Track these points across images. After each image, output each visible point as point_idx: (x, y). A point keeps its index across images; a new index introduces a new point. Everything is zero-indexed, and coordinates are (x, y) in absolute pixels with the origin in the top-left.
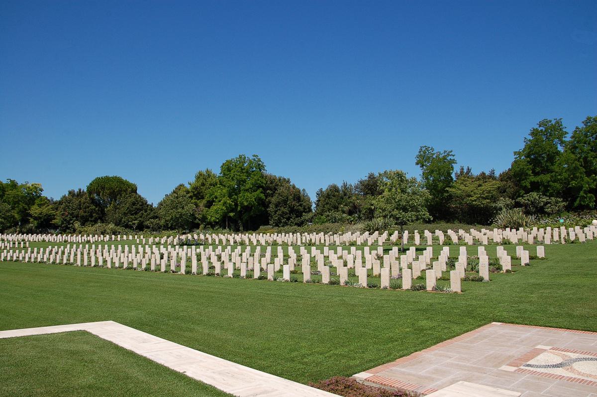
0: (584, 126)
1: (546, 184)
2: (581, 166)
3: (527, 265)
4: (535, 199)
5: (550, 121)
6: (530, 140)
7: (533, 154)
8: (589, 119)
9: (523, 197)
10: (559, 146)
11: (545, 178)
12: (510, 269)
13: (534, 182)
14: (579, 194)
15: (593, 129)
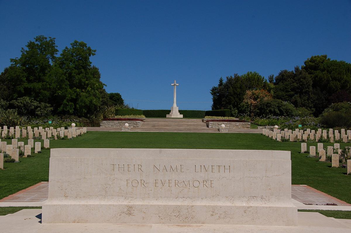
0: (72, 48)
1: (38, 91)
2: (66, 79)
3: (39, 152)
4: (27, 103)
5: (46, 38)
6: (27, 51)
7: (28, 64)
8: (76, 42)
9: (16, 99)
10: (50, 60)
11: (37, 85)
12: (30, 155)
13: (28, 88)
14: (63, 102)
15: (78, 51)
